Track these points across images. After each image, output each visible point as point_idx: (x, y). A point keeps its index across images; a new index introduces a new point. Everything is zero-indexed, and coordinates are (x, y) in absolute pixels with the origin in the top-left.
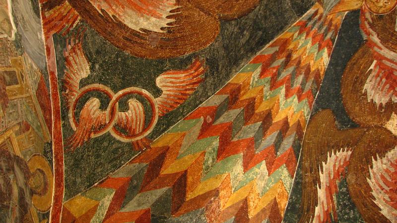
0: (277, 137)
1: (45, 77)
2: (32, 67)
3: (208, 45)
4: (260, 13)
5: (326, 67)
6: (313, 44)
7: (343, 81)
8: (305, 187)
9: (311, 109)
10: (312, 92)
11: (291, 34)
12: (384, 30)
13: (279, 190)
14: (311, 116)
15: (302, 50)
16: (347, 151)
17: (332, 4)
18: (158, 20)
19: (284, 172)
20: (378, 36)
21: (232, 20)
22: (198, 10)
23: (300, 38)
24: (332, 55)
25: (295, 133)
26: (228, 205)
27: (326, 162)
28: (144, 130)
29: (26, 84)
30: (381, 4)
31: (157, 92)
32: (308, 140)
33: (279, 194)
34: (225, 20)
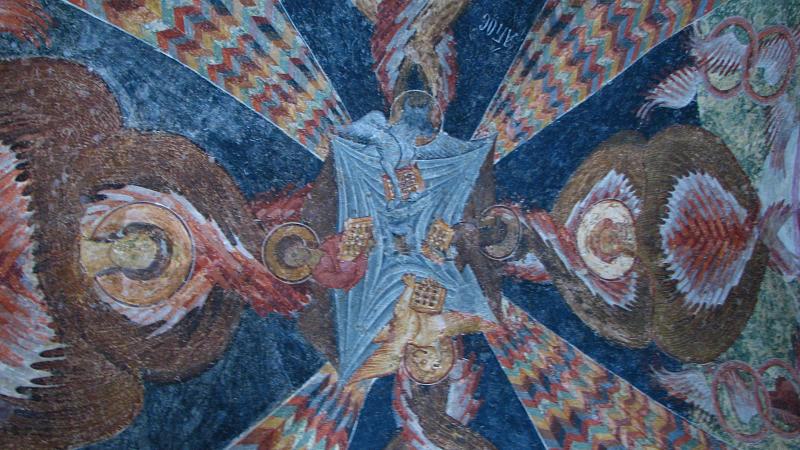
3: (119, 432)
4: (225, 375)
6: (317, 440)
11: (280, 420)
12: (430, 411)
17: (353, 366)
18: (12, 369)
20: (420, 421)
21: (171, 383)
22: (102, 356)
23: (297, 430)
30: (428, 367)
34: (155, 384)
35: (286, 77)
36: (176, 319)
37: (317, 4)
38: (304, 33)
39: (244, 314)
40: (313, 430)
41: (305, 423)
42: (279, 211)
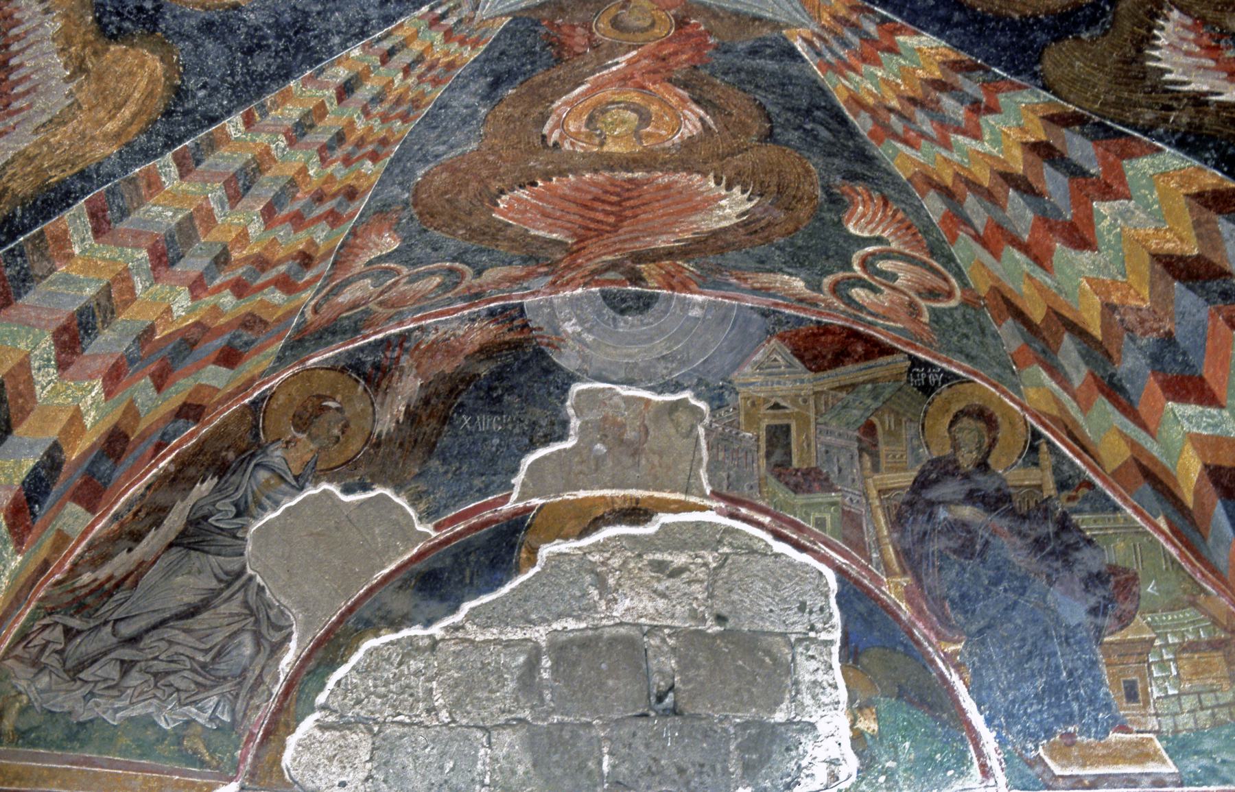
0: (1057, 169)
1: (779, 323)
2: (759, 366)
5: (943, 43)
6: (877, 63)
7: (990, 10)
8: (1200, 127)
9: (1026, 88)
10: (989, 83)
13: (1173, 185)
14: (1045, 88)
15: (886, 88)
16: (1167, 19)
17: (796, 10)
19: (1140, 168)
24: (919, 27)
25: (1064, 131)
26: (1146, 293)
27: (1163, 71)
28: (946, 279)
29: (794, 401)
31: (879, 240)
32: (1095, 102)
33: (1182, 186)
35: (407, 71)
36: (702, 112)
37: (301, 27)
38: (344, 46)
39: (704, 72)
40: (864, 68)
41: (852, 74)
42: (577, 39)
